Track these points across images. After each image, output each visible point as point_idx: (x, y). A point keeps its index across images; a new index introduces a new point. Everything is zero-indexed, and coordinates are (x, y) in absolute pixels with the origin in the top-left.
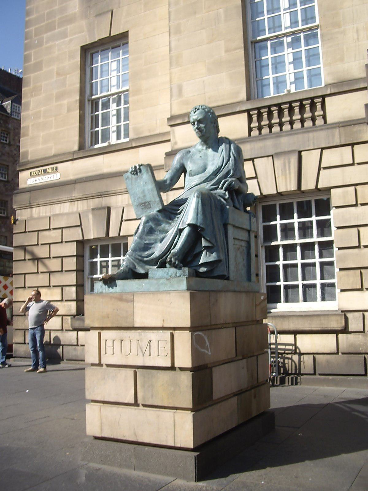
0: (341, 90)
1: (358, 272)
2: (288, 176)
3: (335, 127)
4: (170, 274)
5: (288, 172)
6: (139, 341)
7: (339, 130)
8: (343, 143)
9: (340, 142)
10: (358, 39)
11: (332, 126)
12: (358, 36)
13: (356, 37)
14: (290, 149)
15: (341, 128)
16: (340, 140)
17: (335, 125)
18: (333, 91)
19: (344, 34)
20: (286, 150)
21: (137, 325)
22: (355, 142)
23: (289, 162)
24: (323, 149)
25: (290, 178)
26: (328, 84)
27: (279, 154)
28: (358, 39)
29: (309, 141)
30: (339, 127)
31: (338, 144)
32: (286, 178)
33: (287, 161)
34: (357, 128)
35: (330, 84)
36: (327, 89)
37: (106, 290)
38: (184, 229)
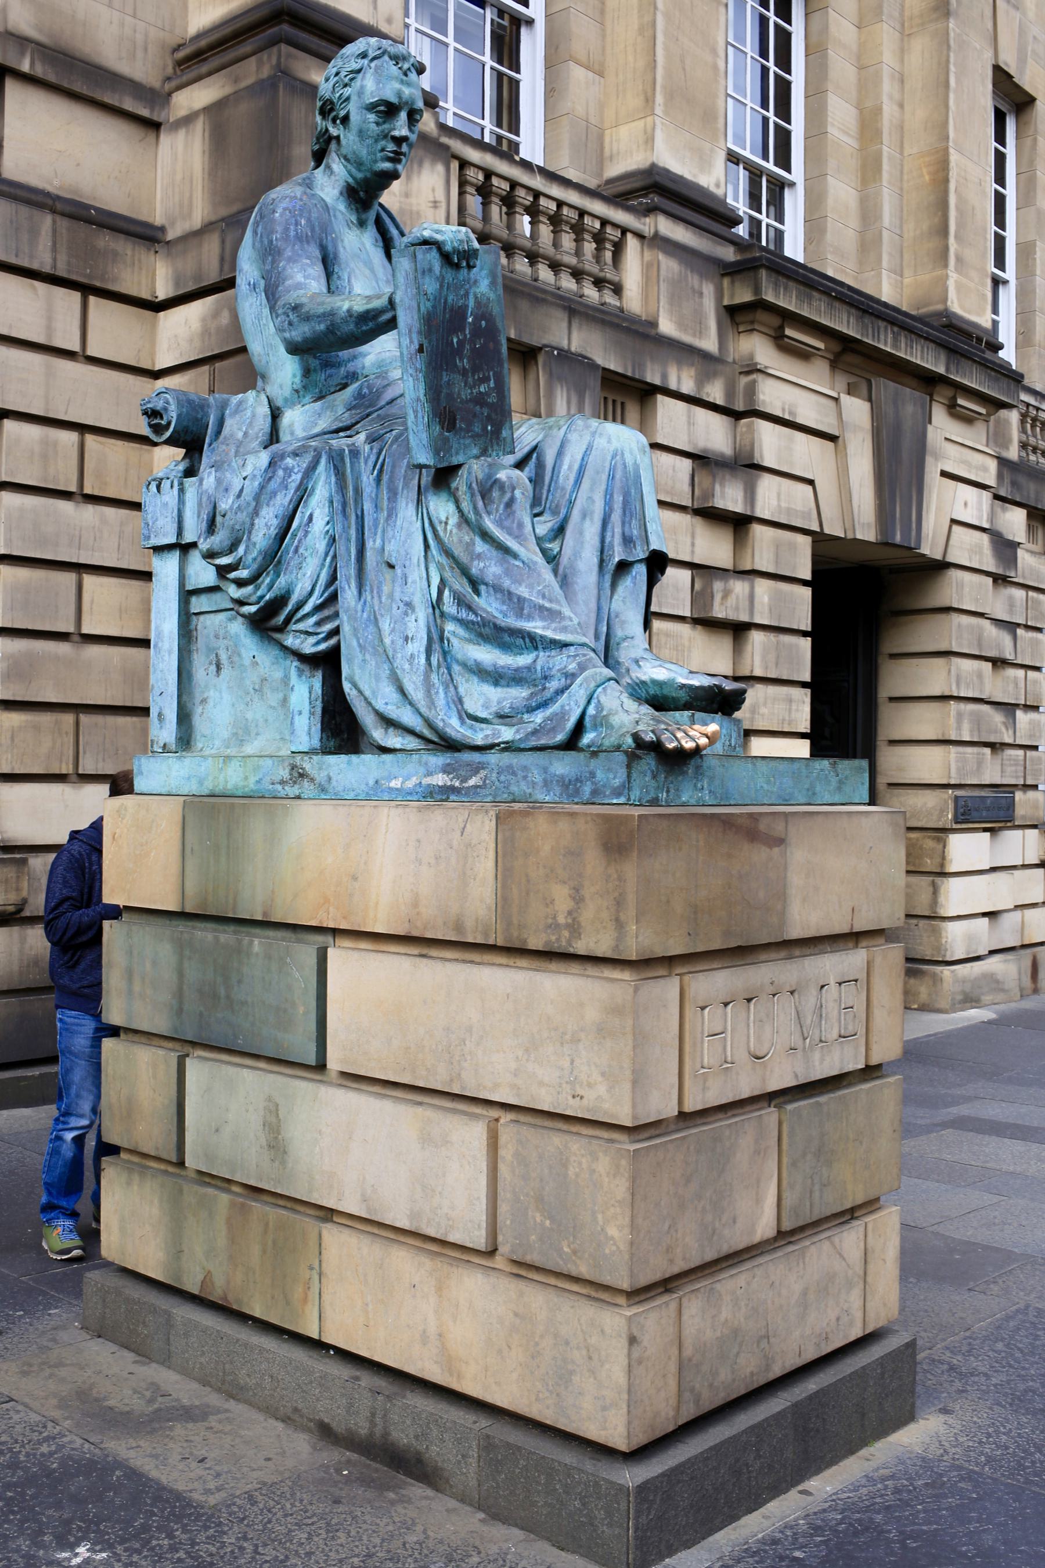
0: (65, 84)
1: (69, 718)
3: (40, 206)
6: (796, 995)
7: (54, 222)
8: (62, 272)
9: (55, 266)
11: (33, 197)
15: (58, 218)
16: (55, 260)
17: (40, 198)
18: (39, 71)
21: (795, 933)
22: (98, 284)
30: (53, 211)
31: (47, 269)
34: (105, 240)
36: (22, 54)
37: (668, 792)
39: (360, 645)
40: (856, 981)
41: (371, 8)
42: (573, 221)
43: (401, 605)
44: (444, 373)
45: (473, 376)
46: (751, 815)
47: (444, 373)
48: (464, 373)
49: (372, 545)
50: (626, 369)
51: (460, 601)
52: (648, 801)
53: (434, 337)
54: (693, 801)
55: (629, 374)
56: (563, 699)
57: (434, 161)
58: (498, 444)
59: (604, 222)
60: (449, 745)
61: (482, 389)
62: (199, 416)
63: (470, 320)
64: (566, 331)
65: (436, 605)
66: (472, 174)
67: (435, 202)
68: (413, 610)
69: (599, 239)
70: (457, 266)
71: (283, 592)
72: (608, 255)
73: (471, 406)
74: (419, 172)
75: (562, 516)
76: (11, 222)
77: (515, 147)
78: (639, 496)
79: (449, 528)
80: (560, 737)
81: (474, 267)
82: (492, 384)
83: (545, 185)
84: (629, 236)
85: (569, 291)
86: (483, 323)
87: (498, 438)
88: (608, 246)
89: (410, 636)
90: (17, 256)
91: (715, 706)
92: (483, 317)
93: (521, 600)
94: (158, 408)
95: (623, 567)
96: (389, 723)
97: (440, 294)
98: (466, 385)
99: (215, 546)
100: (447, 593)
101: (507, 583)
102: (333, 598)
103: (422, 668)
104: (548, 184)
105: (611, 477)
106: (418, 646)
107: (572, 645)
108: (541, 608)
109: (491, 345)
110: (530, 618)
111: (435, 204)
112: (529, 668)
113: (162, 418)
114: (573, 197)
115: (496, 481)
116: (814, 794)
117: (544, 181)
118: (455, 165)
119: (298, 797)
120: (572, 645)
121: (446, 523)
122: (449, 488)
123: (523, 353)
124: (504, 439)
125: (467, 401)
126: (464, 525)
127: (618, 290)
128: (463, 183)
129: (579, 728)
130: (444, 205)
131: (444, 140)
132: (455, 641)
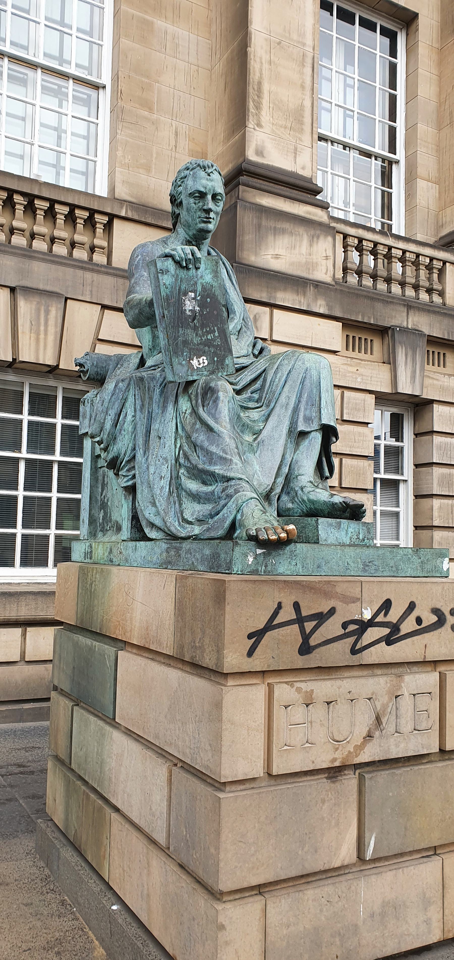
2: (42, 336)
4: (350, 535)
5: (42, 328)
6: (372, 700)
10: (176, 147)
12: (176, 142)
13: (173, 143)
14: (48, 288)
18: (130, 215)
19: (157, 128)
20: (41, 287)
23: (47, 312)
24: (104, 307)
25: (45, 339)
26: (120, 198)
27: (29, 291)
28: (176, 147)
29: (83, 286)
32: (38, 340)
33: (42, 309)
35: (125, 201)
36: (122, 208)
37: (266, 566)
38: (308, 433)
39: (141, 482)
40: (430, 693)
41: (293, 163)
42: (413, 260)
43: (161, 460)
44: (180, 329)
45: (202, 330)
46: (329, 582)
47: (180, 329)
48: (195, 328)
49: (155, 426)
50: (444, 335)
51: (186, 457)
52: (249, 572)
53: (172, 309)
54: (288, 572)
55: (446, 338)
56: (225, 510)
57: (326, 236)
58: (222, 368)
59: (432, 259)
60: (173, 537)
61: (209, 337)
62: (104, 366)
63: (199, 298)
64: (406, 318)
65: (177, 460)
66: (350, 240)
67: (327, 257)
68: (167, 462)
69: (429, 268)
70: (187, 268)
71: (116, 454)
72: (435, 276)
73: (202, 347)
74: (317, 242)
75: (271, 407)
76: (114, 287)
77: (390, 227)
78: (318, 393)
79: (186, 415)
80: (221, 532)
81: (199, 268)
82: (217, 334)
83: (395, 243)
84: (447, 264)
85: (410, 297)
86: (209, 300)
87: (223, 364)
88: (435, 271)
89: (163, 476)
90: (117, 302)
91: (347, 514)
92: (208, 296)
93: (212, 453)
94: (82, 363)
95: (303, 434)
96: (152, 525)
97: (176, 284)
98: (197, 335)
99: (93, 432)
100: (181, 452)
101: (206, 444)
102: (134, 457)
103: (167, 494)
104: (397, 242)
105: (303, 383)
106: (165, 483)
107: (233, 479)
108: (221, 458)
109: (215, 312)
110: (215, 464)
111: (327, 258)
112: (213, 492)
113: (84, 368)
114: (412, 247)
115: (210, 387)
116: (397, 570)
117: (394, 240)
118: (339, 238)
119: (119, 565)
120: (233, 479)
121: (185, 413)
122: (188, 393)
123: (382, 331)
124: (227, 365)
125: (198, 344)
126: (194, 414)
127: (442, 294)
128: (345, 246)
129: (233, 527)
130: (332, 258)
131: (333, 224)
132: (183, 478)
